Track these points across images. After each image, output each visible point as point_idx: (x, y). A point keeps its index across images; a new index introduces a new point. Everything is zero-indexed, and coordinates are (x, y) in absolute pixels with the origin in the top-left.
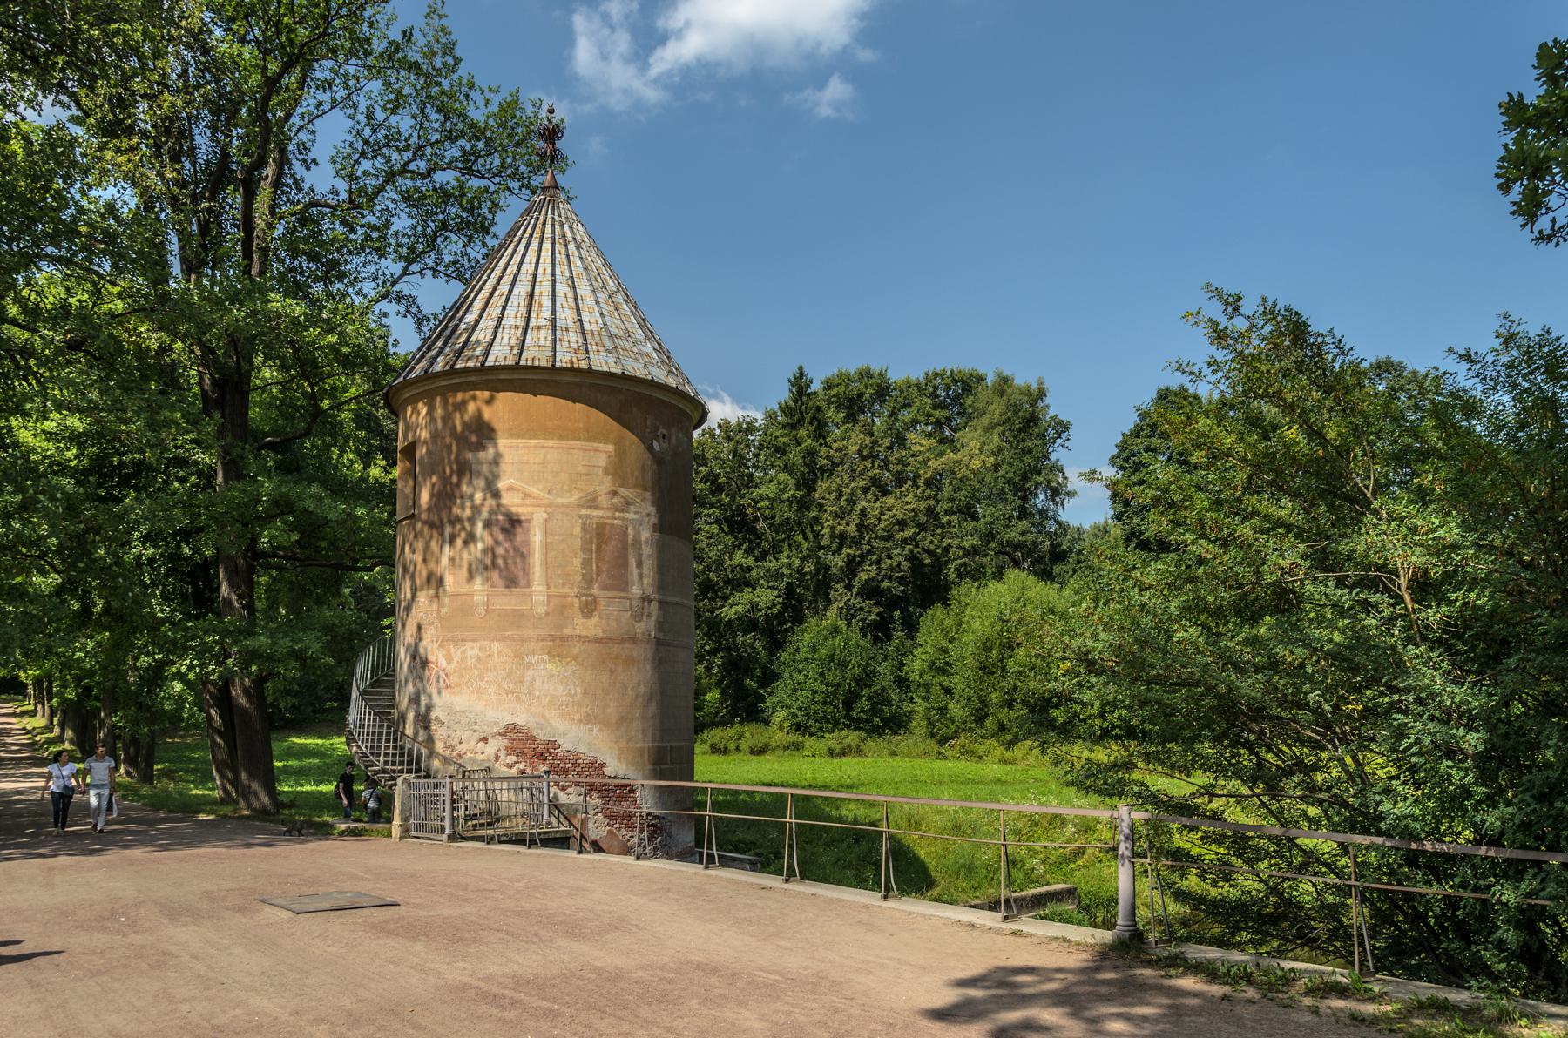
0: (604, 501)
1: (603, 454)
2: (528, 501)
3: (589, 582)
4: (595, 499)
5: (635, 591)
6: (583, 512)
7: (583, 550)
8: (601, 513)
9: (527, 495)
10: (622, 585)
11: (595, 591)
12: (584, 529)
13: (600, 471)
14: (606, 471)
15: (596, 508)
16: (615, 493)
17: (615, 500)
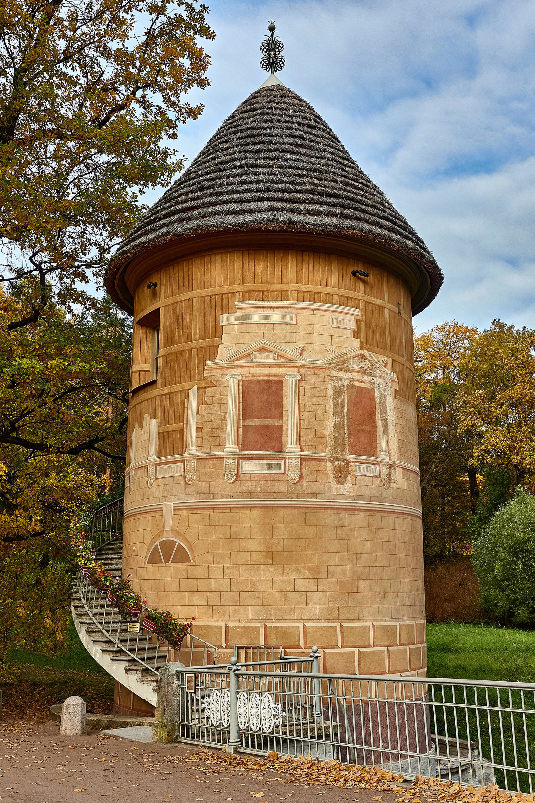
0: (354, 365)
1: (350, 317)
2: (281, 361)
3: (339, 443)
4: (345, 362)
5: (382, 456)
6: (335, 373)
7: (335, 413)
8: (350, 375)
9: (279, 356)
10: (371, 449)
11: (347, 456)
12: (337, 392)
13: (349, 334)
14: (356, 334)
15: (347, 370)
16: (363, 357)
17: (363, 364)
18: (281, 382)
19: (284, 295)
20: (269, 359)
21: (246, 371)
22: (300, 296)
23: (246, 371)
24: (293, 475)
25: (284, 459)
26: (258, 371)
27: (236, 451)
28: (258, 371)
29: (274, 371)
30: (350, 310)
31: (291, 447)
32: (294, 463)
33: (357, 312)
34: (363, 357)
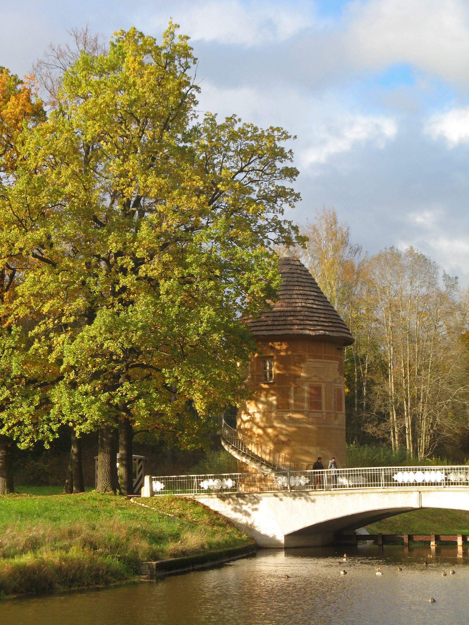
2: (321, 380)
4: (336, 380)
6: (335, 384)
9: (320, 379)
14: (338, 370)
15: (336, 383)
18: (320, 388)
19: (320, 357)
20: (317, 379)
21: (311, 383)
22: (326, 358)
23: (311, 383)
24: (324, 418)
25: (322, 412)
26: (314, 383)
27: (308, 410)
28: (314, 383)
29: (318, 384)
30: (336, 362)
31: (324, 409)
32: (325, 414)
33: (338, 362)
34: (339, 378)
